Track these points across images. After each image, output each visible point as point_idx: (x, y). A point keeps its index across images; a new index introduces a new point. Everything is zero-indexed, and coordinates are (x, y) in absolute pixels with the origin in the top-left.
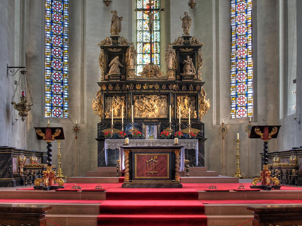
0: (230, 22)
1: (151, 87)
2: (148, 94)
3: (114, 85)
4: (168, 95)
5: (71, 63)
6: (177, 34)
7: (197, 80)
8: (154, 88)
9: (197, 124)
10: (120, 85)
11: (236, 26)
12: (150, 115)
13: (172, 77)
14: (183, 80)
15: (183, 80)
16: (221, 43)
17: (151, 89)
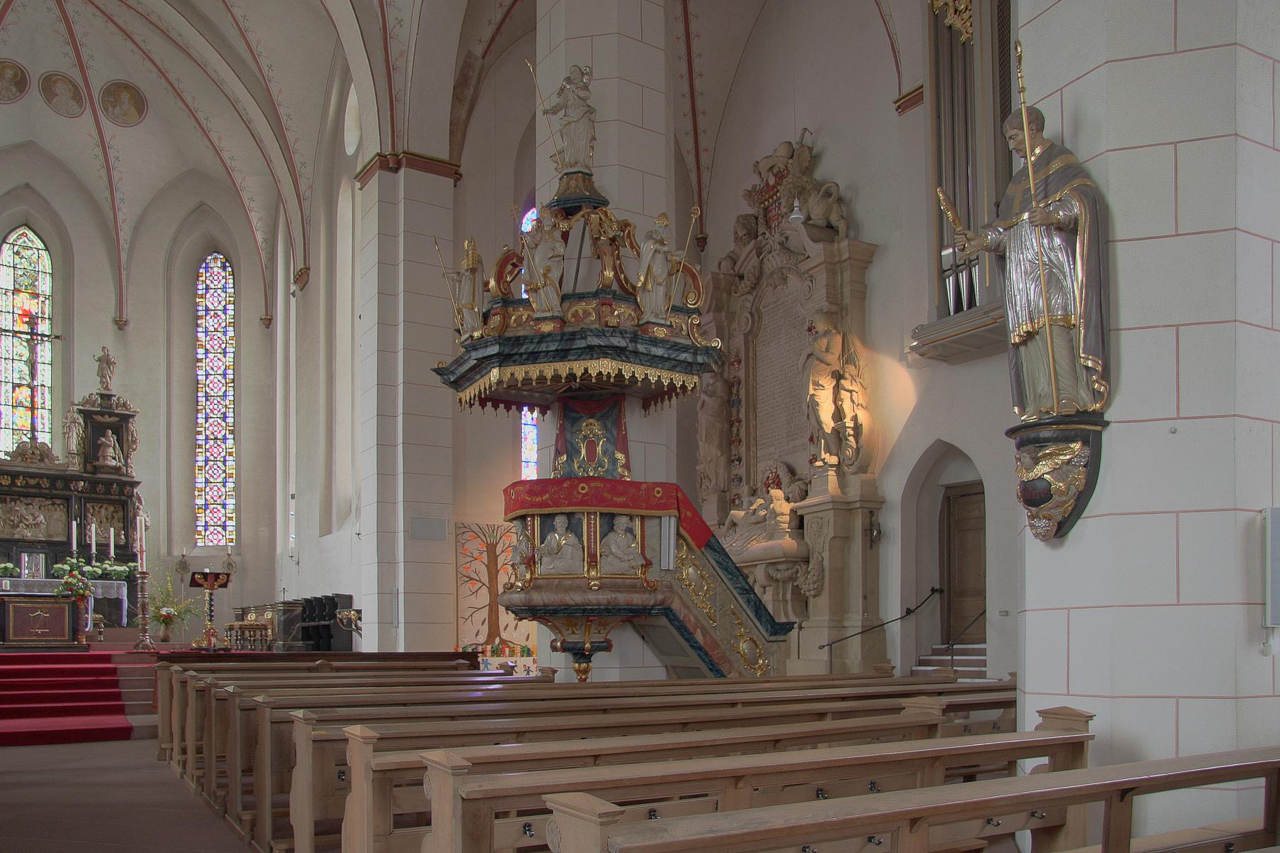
0: (195, 368)
1: (33, 482)
2: (26, 496)
4: (67, 499)
7: (127, 475)
8: (38, 486)
11: (207, 376)
12: (29, 534)
13: (76, 467)
14: (99, 476)
15: (99, 476)
17: (33, 487)
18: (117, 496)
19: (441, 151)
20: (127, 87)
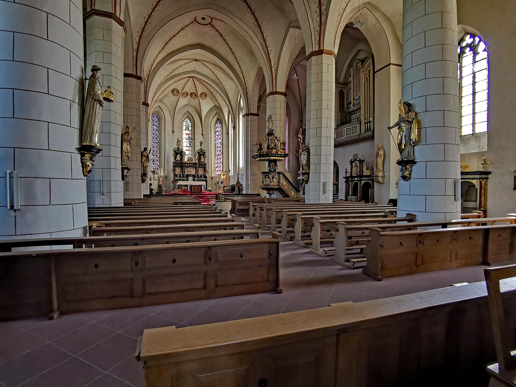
3: (178, 163)
5: (160, 153)
6: (198, 148)
9: (205, 177)
10: (180, 164)
13: (197, 162)
16: (212, 149)
18: (204, 166)
19: (256, 112)
20: (204, 93)
